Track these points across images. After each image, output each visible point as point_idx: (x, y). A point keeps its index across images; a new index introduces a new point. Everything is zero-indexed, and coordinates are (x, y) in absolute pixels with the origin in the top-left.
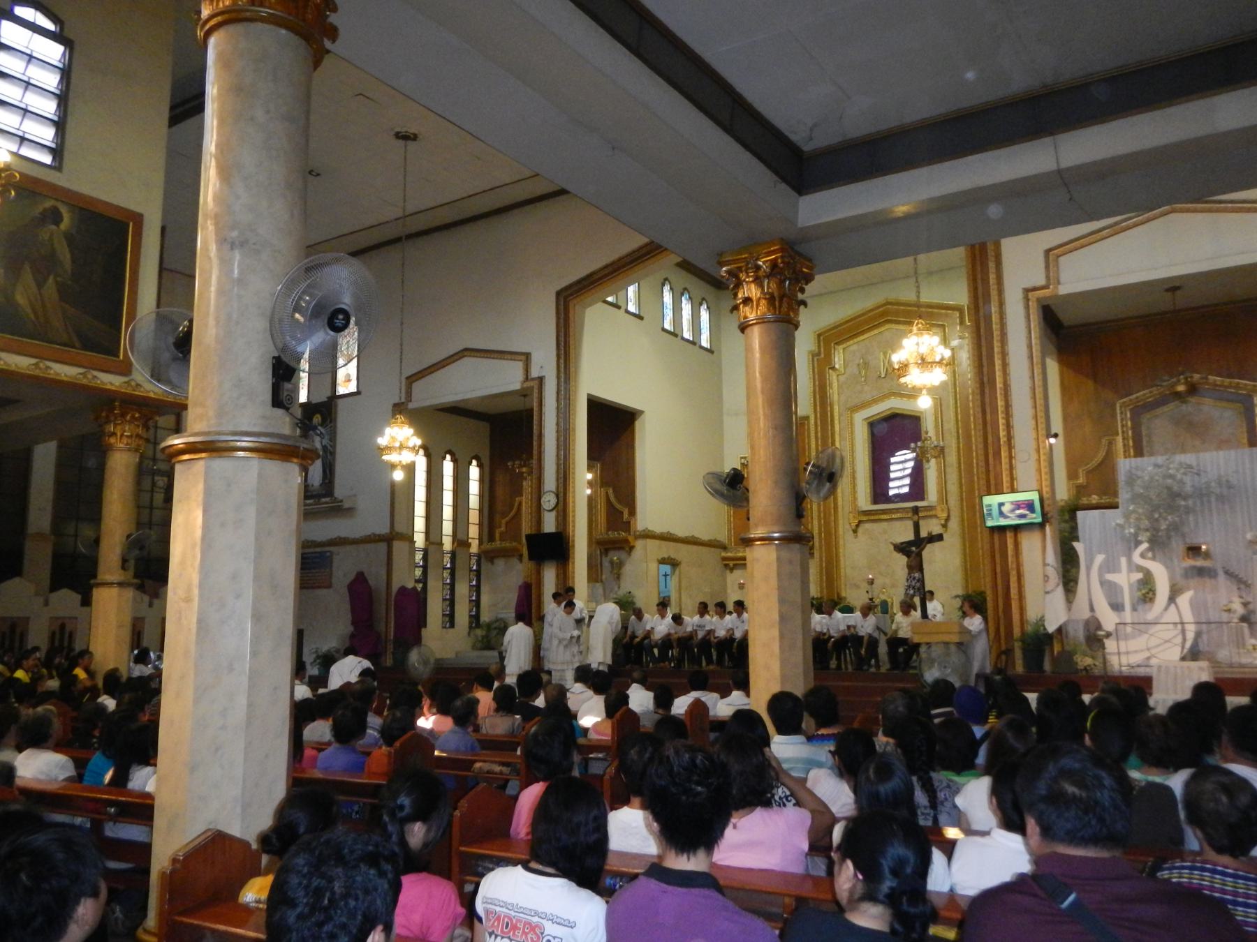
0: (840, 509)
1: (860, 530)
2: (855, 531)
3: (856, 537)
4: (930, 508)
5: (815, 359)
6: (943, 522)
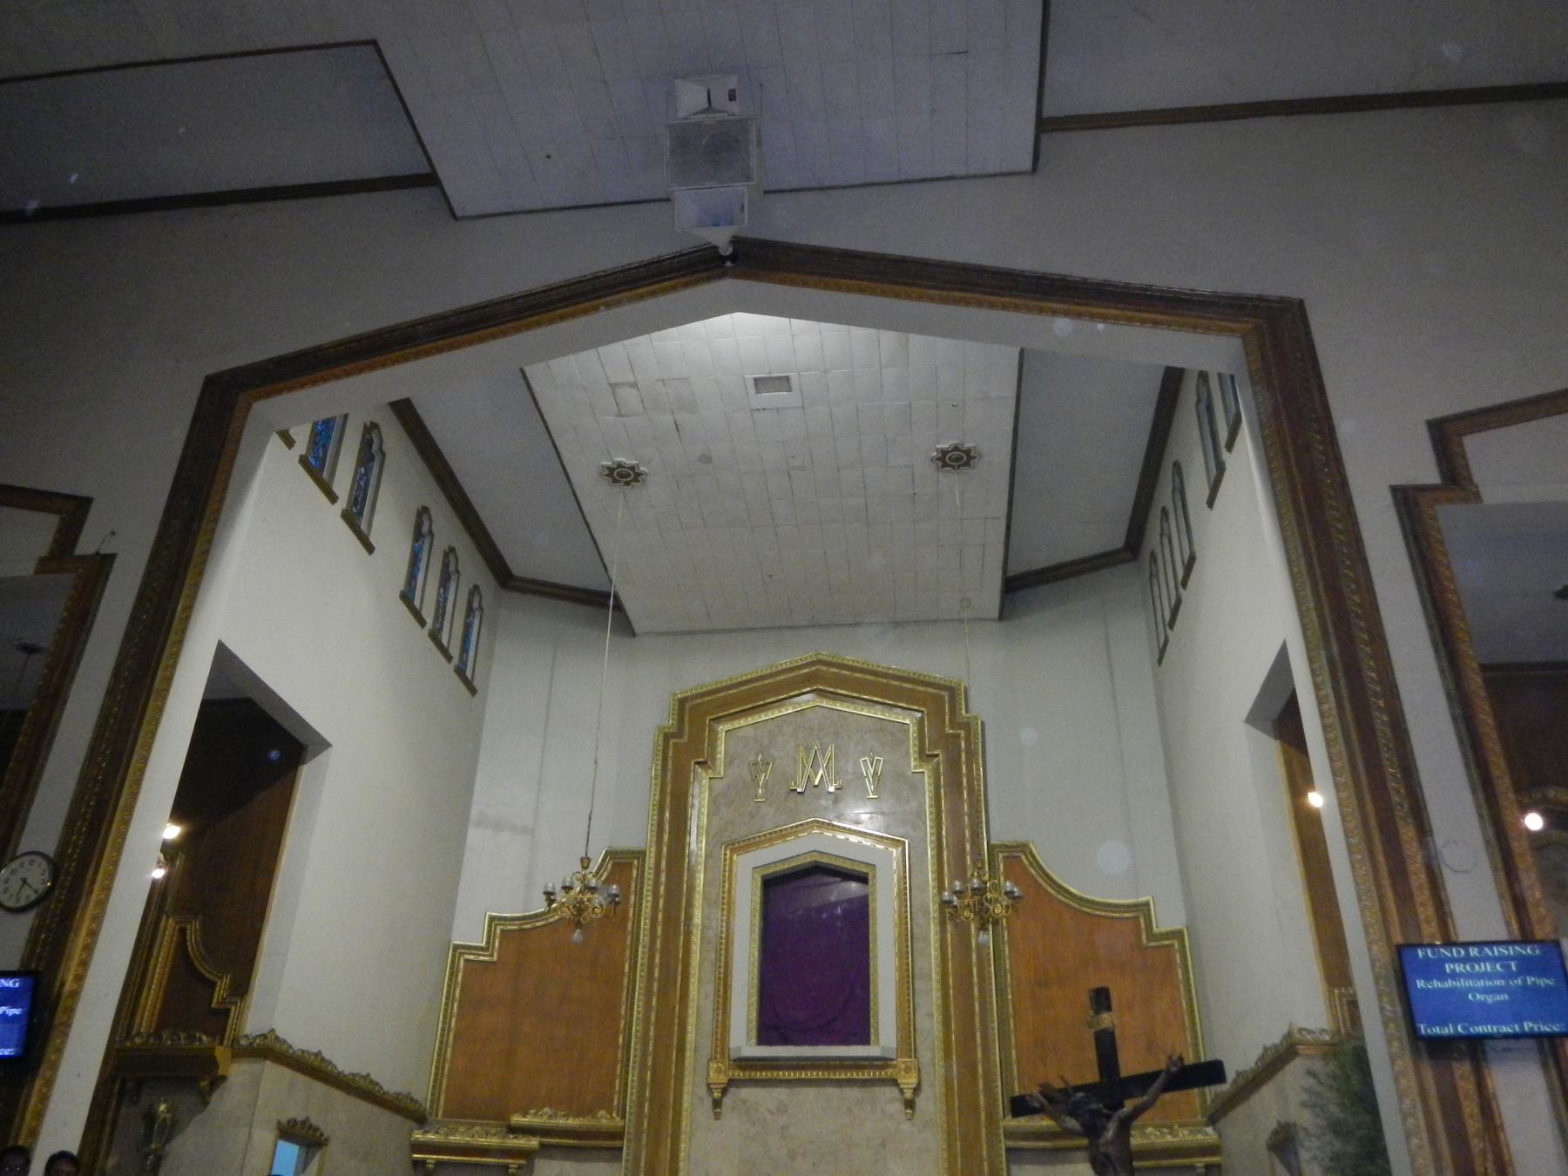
0: (689, 1054)
1: (727, 1101)
2: (717, 1104)
3: (717, 1116)
4: (882, 1062)
5: (672, 741)
6: (909, 1094)
